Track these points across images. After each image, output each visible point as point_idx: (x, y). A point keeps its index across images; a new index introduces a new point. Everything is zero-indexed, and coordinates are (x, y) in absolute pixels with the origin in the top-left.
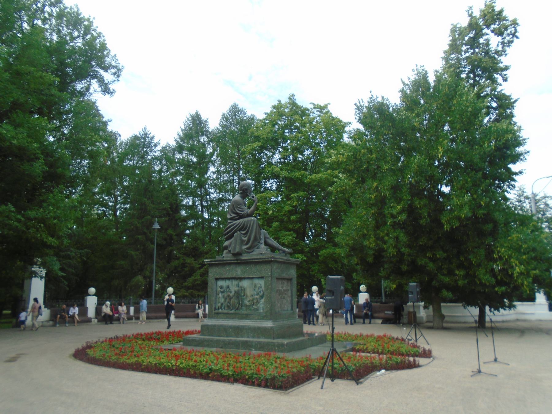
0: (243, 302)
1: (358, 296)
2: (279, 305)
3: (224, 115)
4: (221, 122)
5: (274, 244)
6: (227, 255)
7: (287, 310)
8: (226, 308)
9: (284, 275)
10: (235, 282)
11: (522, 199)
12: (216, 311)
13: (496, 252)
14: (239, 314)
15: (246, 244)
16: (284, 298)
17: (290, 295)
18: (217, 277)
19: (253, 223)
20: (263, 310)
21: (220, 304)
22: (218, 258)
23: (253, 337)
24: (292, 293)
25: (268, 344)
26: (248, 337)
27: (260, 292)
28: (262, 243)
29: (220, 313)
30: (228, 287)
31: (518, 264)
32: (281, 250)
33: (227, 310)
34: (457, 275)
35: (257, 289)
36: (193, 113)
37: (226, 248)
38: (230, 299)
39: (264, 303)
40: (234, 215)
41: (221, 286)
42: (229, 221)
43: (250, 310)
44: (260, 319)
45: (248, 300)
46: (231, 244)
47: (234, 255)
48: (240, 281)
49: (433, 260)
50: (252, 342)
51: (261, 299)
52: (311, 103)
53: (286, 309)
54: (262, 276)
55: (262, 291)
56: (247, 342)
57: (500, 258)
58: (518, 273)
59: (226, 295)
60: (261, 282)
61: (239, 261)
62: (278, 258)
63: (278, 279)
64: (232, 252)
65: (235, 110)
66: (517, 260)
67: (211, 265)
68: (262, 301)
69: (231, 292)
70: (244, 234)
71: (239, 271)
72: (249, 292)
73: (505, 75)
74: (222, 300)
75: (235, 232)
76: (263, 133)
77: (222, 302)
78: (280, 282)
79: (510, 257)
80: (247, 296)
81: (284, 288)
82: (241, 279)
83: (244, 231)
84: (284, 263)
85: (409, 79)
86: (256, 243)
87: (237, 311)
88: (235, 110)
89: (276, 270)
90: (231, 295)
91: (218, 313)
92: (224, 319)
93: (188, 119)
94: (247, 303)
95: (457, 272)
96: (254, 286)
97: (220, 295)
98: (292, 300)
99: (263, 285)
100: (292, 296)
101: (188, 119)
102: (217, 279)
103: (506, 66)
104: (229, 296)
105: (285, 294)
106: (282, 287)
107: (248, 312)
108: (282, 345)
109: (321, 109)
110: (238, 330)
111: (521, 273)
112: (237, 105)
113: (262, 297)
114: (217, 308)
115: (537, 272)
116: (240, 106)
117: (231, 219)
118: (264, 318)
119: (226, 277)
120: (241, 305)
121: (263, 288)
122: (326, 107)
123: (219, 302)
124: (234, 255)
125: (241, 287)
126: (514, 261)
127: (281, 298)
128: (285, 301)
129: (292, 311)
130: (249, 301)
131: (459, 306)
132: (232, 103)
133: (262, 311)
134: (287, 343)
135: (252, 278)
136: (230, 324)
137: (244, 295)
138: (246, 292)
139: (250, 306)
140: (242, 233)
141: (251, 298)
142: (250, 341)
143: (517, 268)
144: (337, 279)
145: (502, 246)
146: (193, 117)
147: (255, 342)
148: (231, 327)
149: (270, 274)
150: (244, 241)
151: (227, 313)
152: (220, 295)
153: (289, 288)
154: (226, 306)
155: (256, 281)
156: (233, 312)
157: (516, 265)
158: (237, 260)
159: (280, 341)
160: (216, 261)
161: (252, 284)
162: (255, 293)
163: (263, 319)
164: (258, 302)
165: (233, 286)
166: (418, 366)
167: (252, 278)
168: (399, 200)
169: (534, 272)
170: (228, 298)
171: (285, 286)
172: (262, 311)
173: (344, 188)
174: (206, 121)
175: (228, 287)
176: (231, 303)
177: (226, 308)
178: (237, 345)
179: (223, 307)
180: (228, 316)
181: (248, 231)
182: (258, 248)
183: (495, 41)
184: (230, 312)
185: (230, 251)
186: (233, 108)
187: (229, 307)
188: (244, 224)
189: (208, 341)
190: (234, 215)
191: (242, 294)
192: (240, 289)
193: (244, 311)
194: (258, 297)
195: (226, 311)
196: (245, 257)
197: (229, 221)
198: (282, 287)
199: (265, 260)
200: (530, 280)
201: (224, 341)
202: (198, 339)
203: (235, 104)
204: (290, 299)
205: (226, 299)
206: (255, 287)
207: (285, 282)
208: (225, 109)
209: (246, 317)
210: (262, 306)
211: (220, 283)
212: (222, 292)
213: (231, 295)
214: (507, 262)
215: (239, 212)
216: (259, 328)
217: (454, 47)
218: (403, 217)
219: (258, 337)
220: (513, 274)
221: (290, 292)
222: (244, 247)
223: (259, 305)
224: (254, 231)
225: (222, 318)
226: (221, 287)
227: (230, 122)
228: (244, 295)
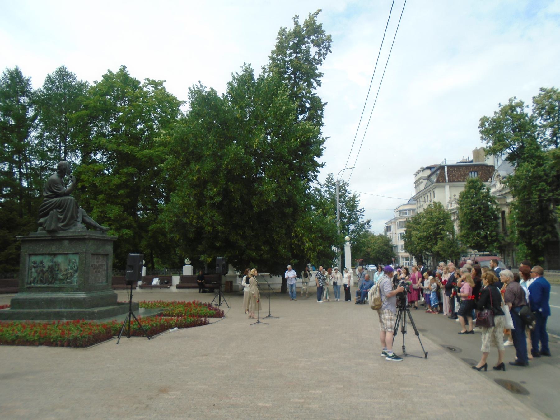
0: (57, 276)
1: (183, 268)
2: (93, 278)
3: (49, 77)
4: (46, 84)
5: (92, 222)
7: (102, 283)
8: (39, 282)
9: (100, 251)
11: (330, 184)
12: (28, 286)
13: (294, 231)
14: (52, 287)
15: (62, 222)
16: (99, 272)
17: (105, 269)
18: (30, 253)
19: (70, 203)
20: (77, 283)
21: (32, 279)
22: (32, 234)
23: (66, 308)
24: (107, 268)
25: (79, 313)
26: (61, 308)
27: (74, 267)
28: (78, 222)
29: (32, 287)
30: (42, 262)
31: (308, 241)
32: (99, 227)
34: (263, 250)
35: (71, 264)
36: (12, 69)
37: (41, 224)
38: (44, 274)
39: (78, 277)
40: (50, 193)
42: (45, 199)
43: (64, 283)
44: (74, 291)
46: (46, 221)
47: (50, 232)
49: (244, 237)
50: (64, 312)
51: (75, 273)
52: (145, 79)
53: (100, 282)
54: (77, 252)
55: (77, 265)
56: (59, 312)
57: (297, 236)
58: (307, 248)
59: (39, 270)
61: (53, 238)
62: (93, 236)
63: (93, 254)
64: (47, 229)
65: (63, 74)
66: (307, 238)
67: (23, 241)
68: (76, 275)
69: (44, 267)
70: (60, 212)
71: (53, 248)
72: (63, 267)
73: (319, 81)
74: (35, 275)
75: (51, 209)
76: (92, 101)
77: (35, 276)
78: (95, 257)
79: (303, 235)
80: (61, 271)
81: (100, 263)
82: (55, 255)
83: (60, 209)
84: (100, 240)
85: (236, 73)
86: (72, 222)
87: (50, 285)
88: (63, 74)
89: (92, 247)
90: (45, 270)
91: (29, 288)
92: (37, 292)
93: (5, 75)
94: (61, 277)
95: (263, 248)
97: (33, 270)
98: (107, 273)
99: (77, 261)
100: (107, 270)
101: (5, 75)
102: (30, 255)
103: (320, 73)
104: (42, 271)
105: (101, 268)
106: (98, 262)
107: (62, 285)
108: (93, 313)
109: (156, 84)
110: (51, 303)
111: (310, 248)
112: (66, 69)
113: (76, 271)
114: (29, 282)
115: (320, 248)
116: (70, 70)
117: (46, 197)
118: (78, 290)
119: (39, 253)
120: (54, 279)
121: (78, 263)
122: (161, 83)
123: (31, 277)
124: (50, 232)
125: (55, 262)
126: (305, 239)
127: (96, 272)
128: (99, 275)
129: (107, 284)
130: (63, 275)
131: (266, 276)
132: (60, 65)
134: (98, 312)
135: (67, 254)
136: (42, 297)
137: (58, 270)
139: (63, 280)
140: (57, 211)
141: (65, 273)
142: (61, 312)
143: (307, 244)
144: (137, 256)
145: (299, 226)
146: (11, 74)
147: (67, 312)
148: (43, 300)
149: (84, 250)
150: (61, 219)
151: (40, 287)
152: (33, 270)
153: (105, 263)
155: (71, 257)
157: (307, 242)
158: (52, 237)
159: (90, 310)
160: (30, 237)
162: (69, 267)
163: (76, 291)
164: (72, 276)
165: (47, 262)
166: (208, 323)
167: (67, 254)
168: (216, 184)
169: (320, 248)
171: (101, 261)
172: (75, 284)
173: (174, 166)
174: (28, 80)
175: (42, 262)
176: (44, 277)
177: (39, 282)
178: (48, 316)
179: (35, 282)
181: (65, 209)
182: (74, 226)
183: (314, 50)
184: (43, 285)
185: (44, 228)
186: (61, 71)
188: (61, 203)
189: (17, 313)
190: (50, 193)
192: (54, 264)
193: (57, 285)
194: (72, 271)
195: (39, 285)
196: (61, 234)
197: (45, 199)
198: (98, 262)
199: (79, 237)
200: (315, 254)
203: (63, 67)
204: (105, 272)
205: (39, 274)
207: (101, 257)
208: (52, 71)
209: (60, 290)
210: (75, 279)
211: (33, 258)
212: (35, 267)
213: (45, 270)
214: (300, 240)
215: (56, 191)
216: (72, 300)
217: (281, 49)
218: (218, 199)
219: (71, 308)
220: (304, 249)
221: (106, 266)
222: (61, 225)
223: (72, 279)
224: (71, 209)
226: (35, 263)
227: (57, 86)
228: (58, 270)
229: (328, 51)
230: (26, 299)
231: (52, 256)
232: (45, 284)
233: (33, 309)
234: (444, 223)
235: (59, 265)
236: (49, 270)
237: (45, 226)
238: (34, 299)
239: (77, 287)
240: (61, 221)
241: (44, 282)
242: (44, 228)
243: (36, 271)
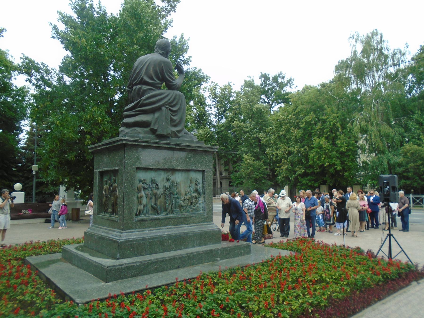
0: (176, 202)
6: (147, 135)
8: (150, 212)
10: (163, 175)
14: (175, 218)
15: (175, 126)
20: (203, 210)
21: (142, 207)
23: (200, 246)
26: (194, 246)
29: (146, 220)
33: (151, 214)
38: (156, 199)
41: (144, 180)
43: (188, 211)
44: (201, 222)
45: (183, 198)
48: (172, 174)
56: (211, 251)
60: (199, 177)
69: (158, 189)
72: (183, 189)
80: (181, 194)
82: (174, 171)
91: (142, 221)
94: (183, 204)
96: (189, 182)
97: (143, 193)
104: (155, 195)
133: (202, 212)
138: (179, 189)
141: (187, 197)
142: (215, 250)
148: (170, 237)
154: (150, 208)
155: (193, 175)
156: (163, 216)
158: (176, 145)
160: (140, 142)
161: (188, 178)
162: (192, 190)
163: (205, 221)
170: (154, 197)
172: (202, 212)
176: (158, 203)
179: (145, 212)
180: (160, 223)
187: (155, 210)
189: (156, 262)
191: (176, 192)
194: (195, 194)
195: (155, 217)
201: (181, 258)
202: (138, 264)
206: (191, 182)
209: (185, 221)
210: (202, 206)
211: (142, 175)
216: (206, 233)
219: (206, 244)
222: (175, 129)
223: (197, 205)
225: (149, 227)
226: (144, 182)
229: (173, 10)
230: (145, 239)
231: (170, 173)
232: (161, 213)
233: (156, 253)
234: (235, 162)
235: (177, 185)
236: (167, 193)
237: (156, 128)
238: (155, 238)
239: (206, 216)
240: (175, 124)
241: (159, 212)
242: (153, 131)
243: (147, 195)
